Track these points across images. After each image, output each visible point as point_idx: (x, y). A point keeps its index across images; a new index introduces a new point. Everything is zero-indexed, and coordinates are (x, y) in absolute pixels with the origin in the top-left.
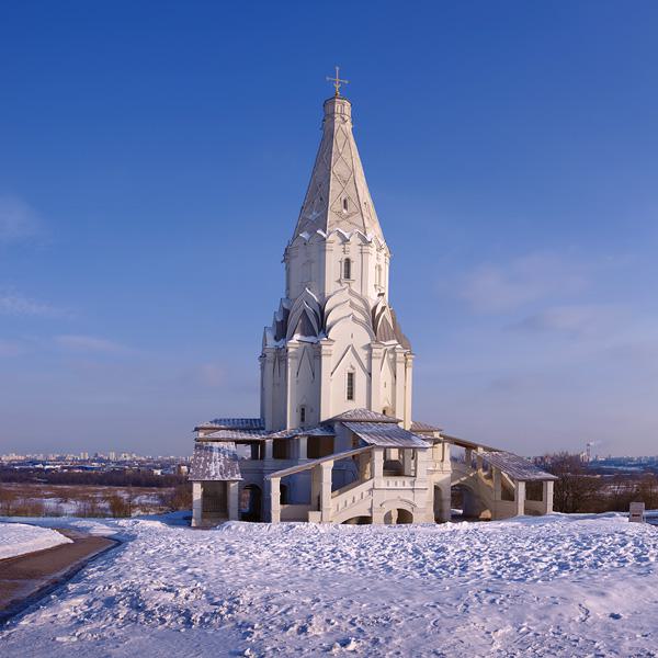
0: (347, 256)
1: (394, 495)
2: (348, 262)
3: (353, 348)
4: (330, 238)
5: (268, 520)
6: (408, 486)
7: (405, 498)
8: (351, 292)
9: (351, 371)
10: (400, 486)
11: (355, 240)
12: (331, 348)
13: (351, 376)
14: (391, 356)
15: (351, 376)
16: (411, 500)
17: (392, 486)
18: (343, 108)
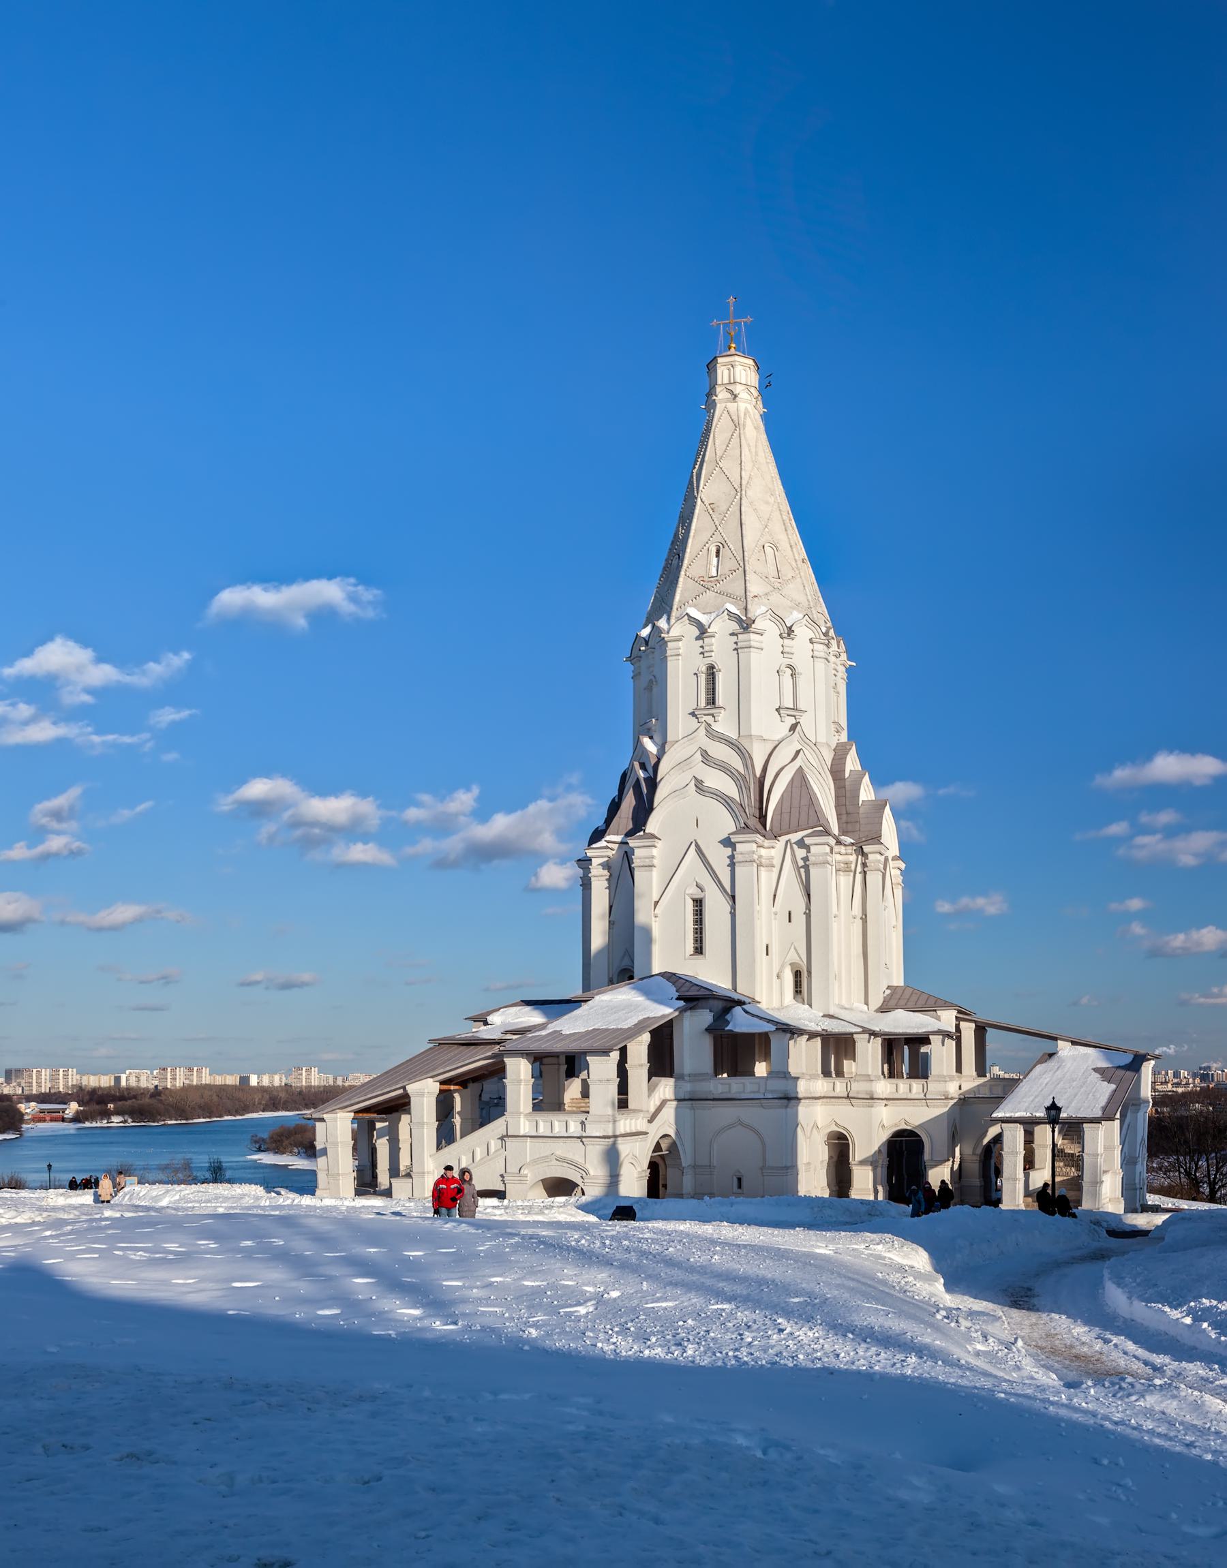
0: (708, 661)
1: (546, 1147)
2: (711, 672)
3: (697, 846)
4: (674, 632)
5: (314, 1173)
6: (574, 1128)
7: (570, 1156)
8: (711, 734)
9: (699, 895)
10: (558, 1129)
11: (721, 627)
12: (655, 852)
13: (699, 903)
14: (801, 853)
15: (699, 903)
16: (580, 1160)
17: (543, 1129)
18: (739, 374)
